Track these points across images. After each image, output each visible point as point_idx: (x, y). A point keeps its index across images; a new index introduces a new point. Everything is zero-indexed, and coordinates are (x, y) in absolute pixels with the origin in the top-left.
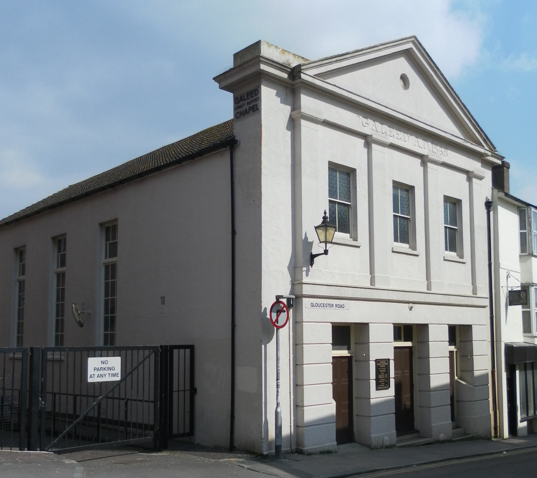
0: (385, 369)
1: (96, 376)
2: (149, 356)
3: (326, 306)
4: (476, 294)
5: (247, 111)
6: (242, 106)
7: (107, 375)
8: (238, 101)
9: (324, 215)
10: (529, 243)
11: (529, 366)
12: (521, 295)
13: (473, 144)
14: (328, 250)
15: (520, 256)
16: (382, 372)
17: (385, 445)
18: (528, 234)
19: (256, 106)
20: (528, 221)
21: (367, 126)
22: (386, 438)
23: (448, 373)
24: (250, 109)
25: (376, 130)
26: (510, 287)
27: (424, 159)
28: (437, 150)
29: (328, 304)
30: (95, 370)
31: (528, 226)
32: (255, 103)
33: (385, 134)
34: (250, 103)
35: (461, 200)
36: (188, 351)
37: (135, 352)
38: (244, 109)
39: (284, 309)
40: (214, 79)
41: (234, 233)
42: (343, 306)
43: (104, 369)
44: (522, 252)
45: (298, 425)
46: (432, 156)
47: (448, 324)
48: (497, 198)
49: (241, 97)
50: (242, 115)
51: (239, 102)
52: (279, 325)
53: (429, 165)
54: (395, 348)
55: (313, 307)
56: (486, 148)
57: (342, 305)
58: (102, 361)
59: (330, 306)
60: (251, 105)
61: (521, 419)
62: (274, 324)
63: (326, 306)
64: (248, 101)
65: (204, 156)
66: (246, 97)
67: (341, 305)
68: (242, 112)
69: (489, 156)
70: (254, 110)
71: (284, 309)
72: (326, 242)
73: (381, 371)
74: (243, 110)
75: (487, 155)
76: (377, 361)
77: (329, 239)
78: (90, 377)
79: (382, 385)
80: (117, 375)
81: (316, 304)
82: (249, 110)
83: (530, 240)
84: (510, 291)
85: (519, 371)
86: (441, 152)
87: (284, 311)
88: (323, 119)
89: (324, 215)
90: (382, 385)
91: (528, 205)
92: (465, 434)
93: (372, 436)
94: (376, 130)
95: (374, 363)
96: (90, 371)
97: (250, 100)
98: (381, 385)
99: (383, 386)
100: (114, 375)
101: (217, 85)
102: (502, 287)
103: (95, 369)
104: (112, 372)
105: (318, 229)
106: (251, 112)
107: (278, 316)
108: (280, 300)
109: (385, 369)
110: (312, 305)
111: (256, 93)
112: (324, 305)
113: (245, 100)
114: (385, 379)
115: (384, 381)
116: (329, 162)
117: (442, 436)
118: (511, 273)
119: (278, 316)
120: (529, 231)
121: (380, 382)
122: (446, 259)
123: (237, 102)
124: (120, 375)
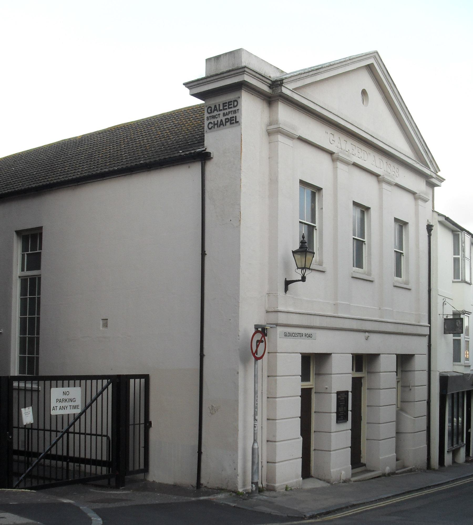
1: (58, 408)
2: (107, 387)
5: (223, 123)
7: (69, 407)
8: (211, 110)
10: (462, 268)
12: (457, 323)
13: (423, 166)
14: (305, 277)
16: (342, 405)
17: (343, 480)
18: (462, 259)
20: (462, 246)
22: (343, 472)
25: (340, 147)
26: (446, 315)
29: (299, 334)
30: (57, 401)
32: (234, 115)
34: (227, 114)
36: (143, 380)
37: (94, 382)
40: (184, 84)
41: (203, 254)
43: (66, 400)
49: (215, 106)
50: (216, 126)
51: (211, 112)
52: (259, 355)
55: (286, 337)
56: (432, 170)
58: (64, 392)
60: (229, 117)
61: (448, 450)
66: (221, 108)
68: (216, 123)
69: (433, 178)
72: (304, 268)
73: (341, 404)
74: (218, 121)
76: (338, 393)
78: (53, 409)
80: (78, 407)
82: (226, 122)
83: (463, 266)
84: (445, 319)
91: (462, 229)
92: (404, 467)
93: (332, 470)
96: (53, 403)
99: (342, 420)
100: (75, 407)
101: (187, 91)
102: (439, 314)
103: (58, 400)
104: (72, 404)
106: (228, 123)
110: (286, 335)
111: (235, 104)
112: (295, 335)
113: (220, 110)
117: (388, 469)
120: (463, 256)
123: (209, 111)
124: (80, 407)
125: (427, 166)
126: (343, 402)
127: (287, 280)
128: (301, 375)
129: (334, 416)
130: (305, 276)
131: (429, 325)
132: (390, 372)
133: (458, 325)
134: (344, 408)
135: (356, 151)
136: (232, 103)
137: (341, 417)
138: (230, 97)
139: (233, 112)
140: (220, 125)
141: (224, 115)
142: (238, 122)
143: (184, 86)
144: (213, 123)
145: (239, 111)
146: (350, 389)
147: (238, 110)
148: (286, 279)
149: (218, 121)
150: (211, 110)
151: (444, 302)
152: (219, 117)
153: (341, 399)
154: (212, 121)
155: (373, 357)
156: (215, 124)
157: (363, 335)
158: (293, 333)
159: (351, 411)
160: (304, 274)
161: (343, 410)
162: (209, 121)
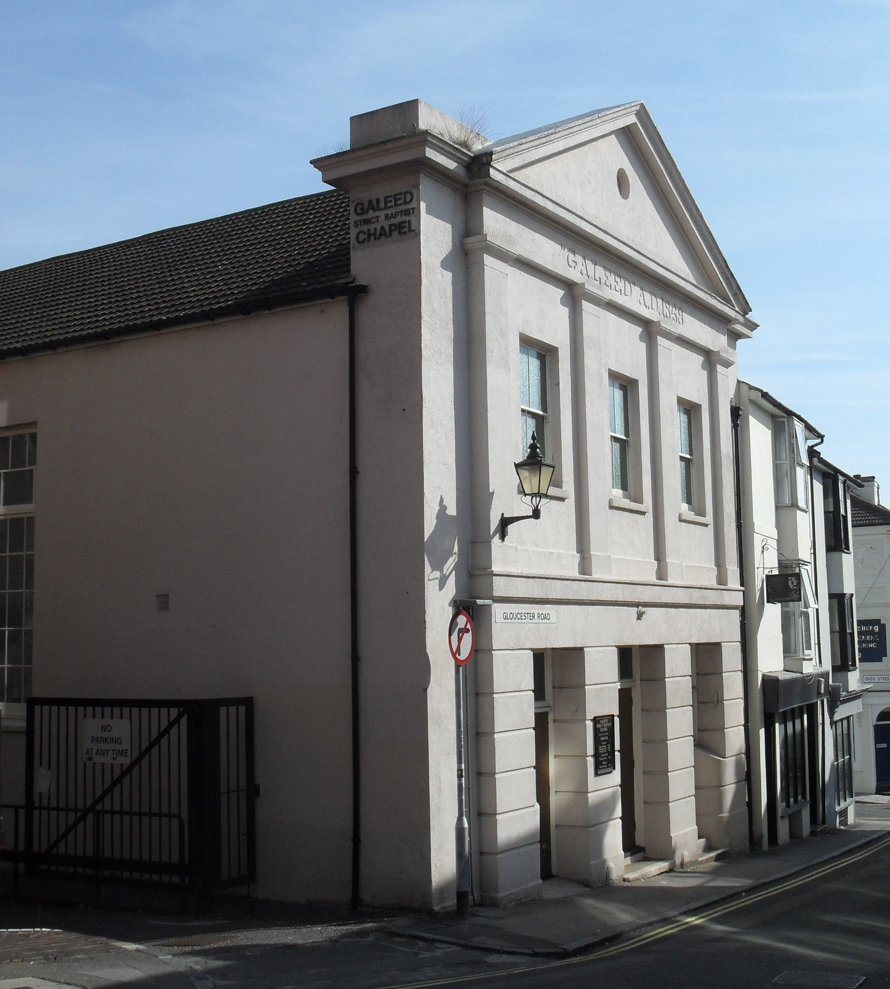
0: (607, 734)
3: (525, 618)
4: (725, 584)
6: (373, 220)
8: (362, 209)
11: (789, 716)
12: (790, 582)
16: (604, 741)
19: (407, 224)
21: (575, 267)
23: (690, 736)
24: (393, 228)
28: (669, 311)
29: (528, 614)
31: (790, 454)
32: (406, 218)
33: (598, 282)
34: (393, 216)
35: (701, 405)
38: (378, 226)
39: (467, 627)
40: (311, 162)
41: (354, 472)
45: (484, 851)
46: (666, 325)
48: (748, 401)
49: (370, 202)
51: (363, 212)
53: (661, 340)
57: (547, 614)
60: (393, 221)
63: (525, 618)
64: (389, 212)
66: (382, 205)
68: (372, 231)
70: (403, 230)
71: (467, 627)
73: (602, 739)
74: (375, 229)
75: (737, 321)
76: (596, 720)
79: (604, 766)
81: (511, 615)
82: (391, 231)
84: (767, 576)
85: (779, 724)
87: (467, 631)
90: (604, 765)
91: (790, 414)
93: (590, 863)
95: (591, 724)
97: (393, 211)
98: (602, 765)
99: (605, 768)
107: (460, 640)
109: (607, 734)
113: (381, 210)
114: (607, 755)
115: (606, 758)
119: (460, 640)
121: (602, 759)
123: (359, 211)
126: (606, 735)
127: (505, 516)
128: (533, 689)
129: (590, 761)
130: (539, 508)
131: (743, 588)
132: (681, 676)
133: (791, 587)
134: (607, 747)
135: (612, 278)
136: (402, 196)
137: (604, 763)
138: (397, 186)
139: (403, 213)
140: (381, 235)
141: (387, 217)
142: (414, 231)
143: (312, 165)
144: (366, 231)
145: (415, 211)
146: (616, 712)
147: (413, 209)
148: (503, 514)
149: (375, 229)
150: (362, 209)
151: (765, 545)
152: (378, 221)
153: (602, 730)
154: (365, 228)
155: (655, 652)
156: (369, 235)
159: (619, 751)
160: (537, 507)
161: (606, 751)
162: (358, 230)
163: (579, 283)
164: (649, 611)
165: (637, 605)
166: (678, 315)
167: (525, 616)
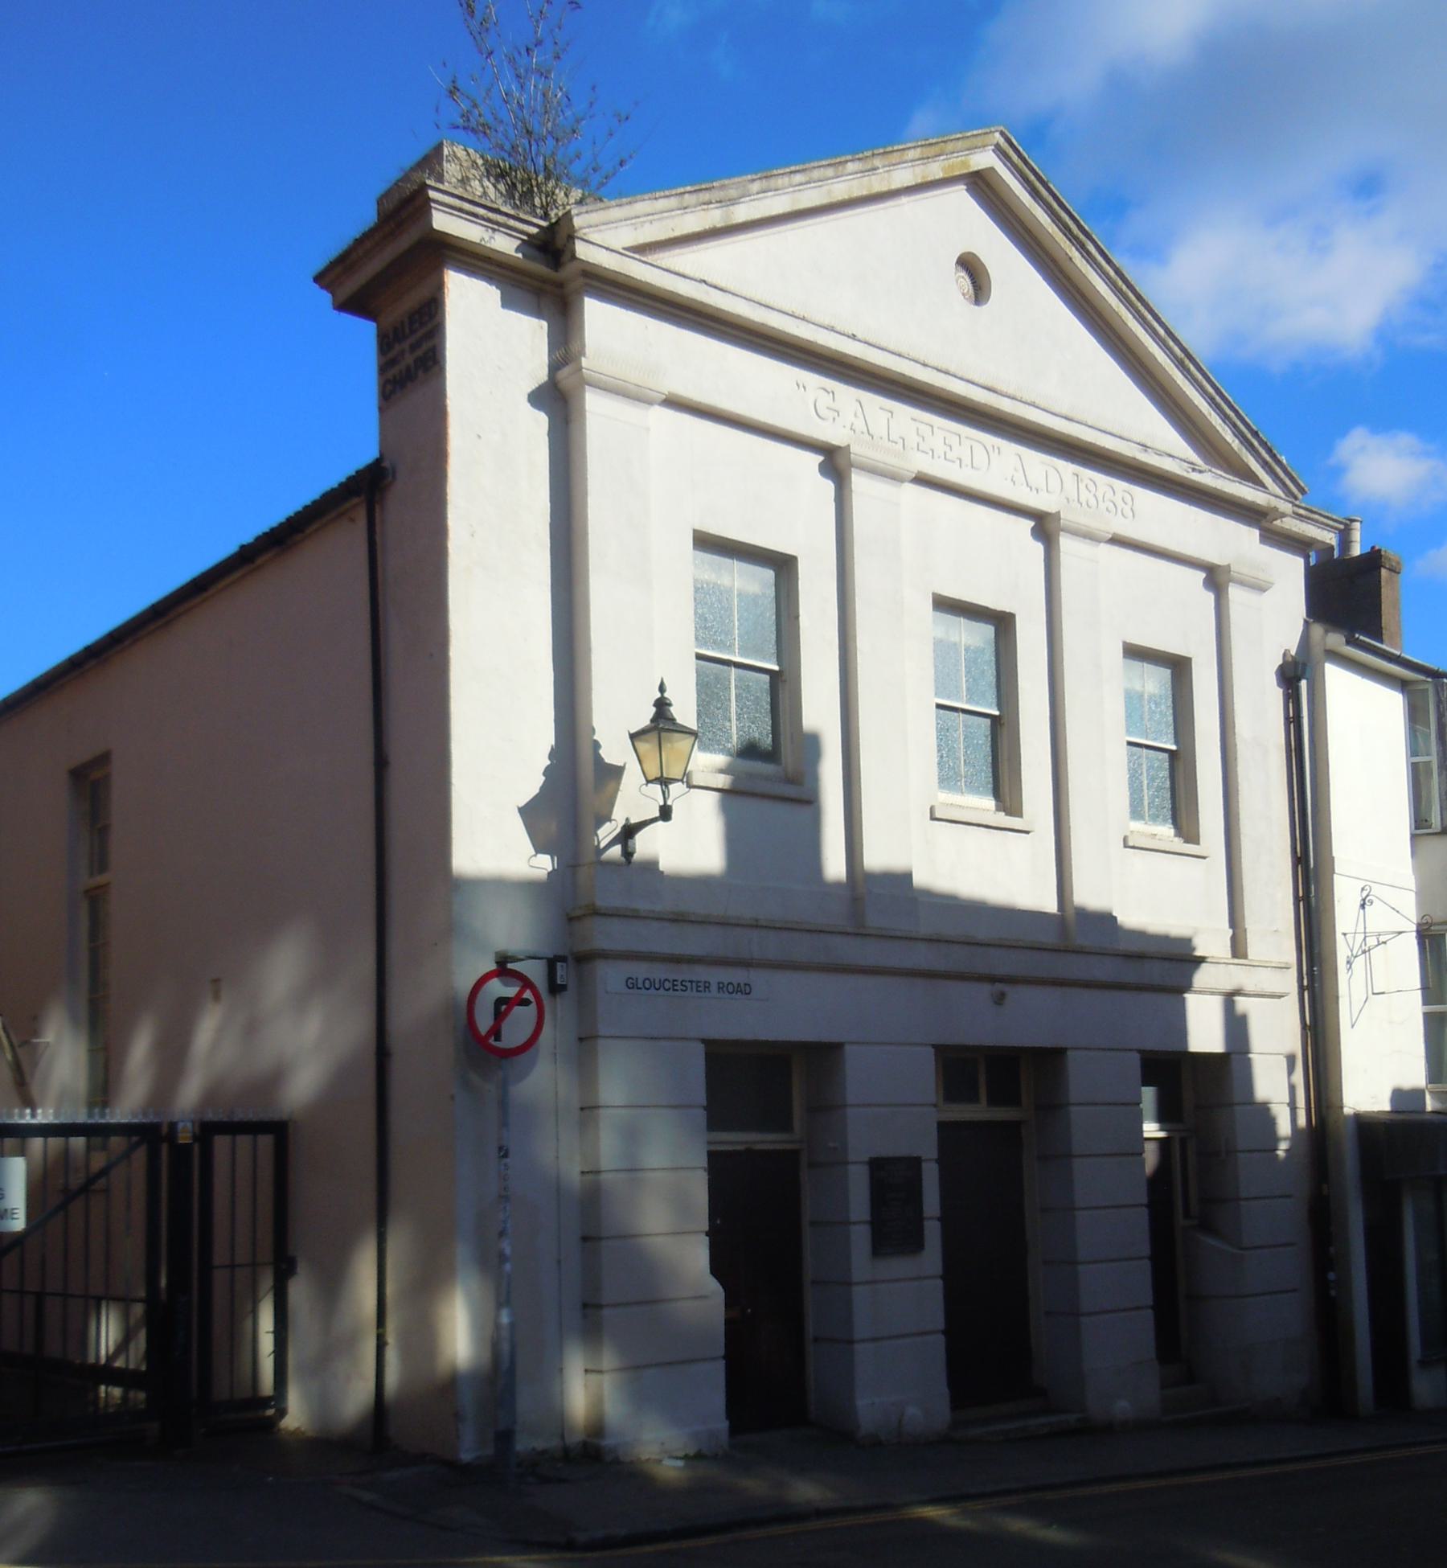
4: (1245, 957)
9: (659, 695)
15: (1413, 837)
21: (834, 419)
25: (865, 430)
27: (1045, 527)
28: (1095, 496)
29: (691, 982)
36: (266, 1141)
41: (381, 763)
42: (747, 987)
44: (1417, 828)
47: (1139, 1051)
54: (943, 1126)
55: (635, 991)
59: (699, 989)
62: (481, 1041)
63: (684, 988)
65: (308, 531)
67: (739, 984)
69: (1283, 515)
72: (664, 782)
77: (674, 772)
81: (647, 981)
86: (1111, 506)
87: (526, 1002)
88: (667, 393)
89: (659, 695)
94: (868, 430)
102: (1345, 934)
105: (640, 741)
108: (510, 966)
110: (632, 984)
112: (674, 985)
116: (695, 531)
118: (1376, 890)
122: (1131, 844)
125: (1249, 477)
129: (860, 1237)
151: (1367, 896)
157: (985, 990)
158: (666, 980)
163: (842, 445)
164: (1014, 993)
165: (993, 979)
166: (1120, 504)
167: (685, 986)
